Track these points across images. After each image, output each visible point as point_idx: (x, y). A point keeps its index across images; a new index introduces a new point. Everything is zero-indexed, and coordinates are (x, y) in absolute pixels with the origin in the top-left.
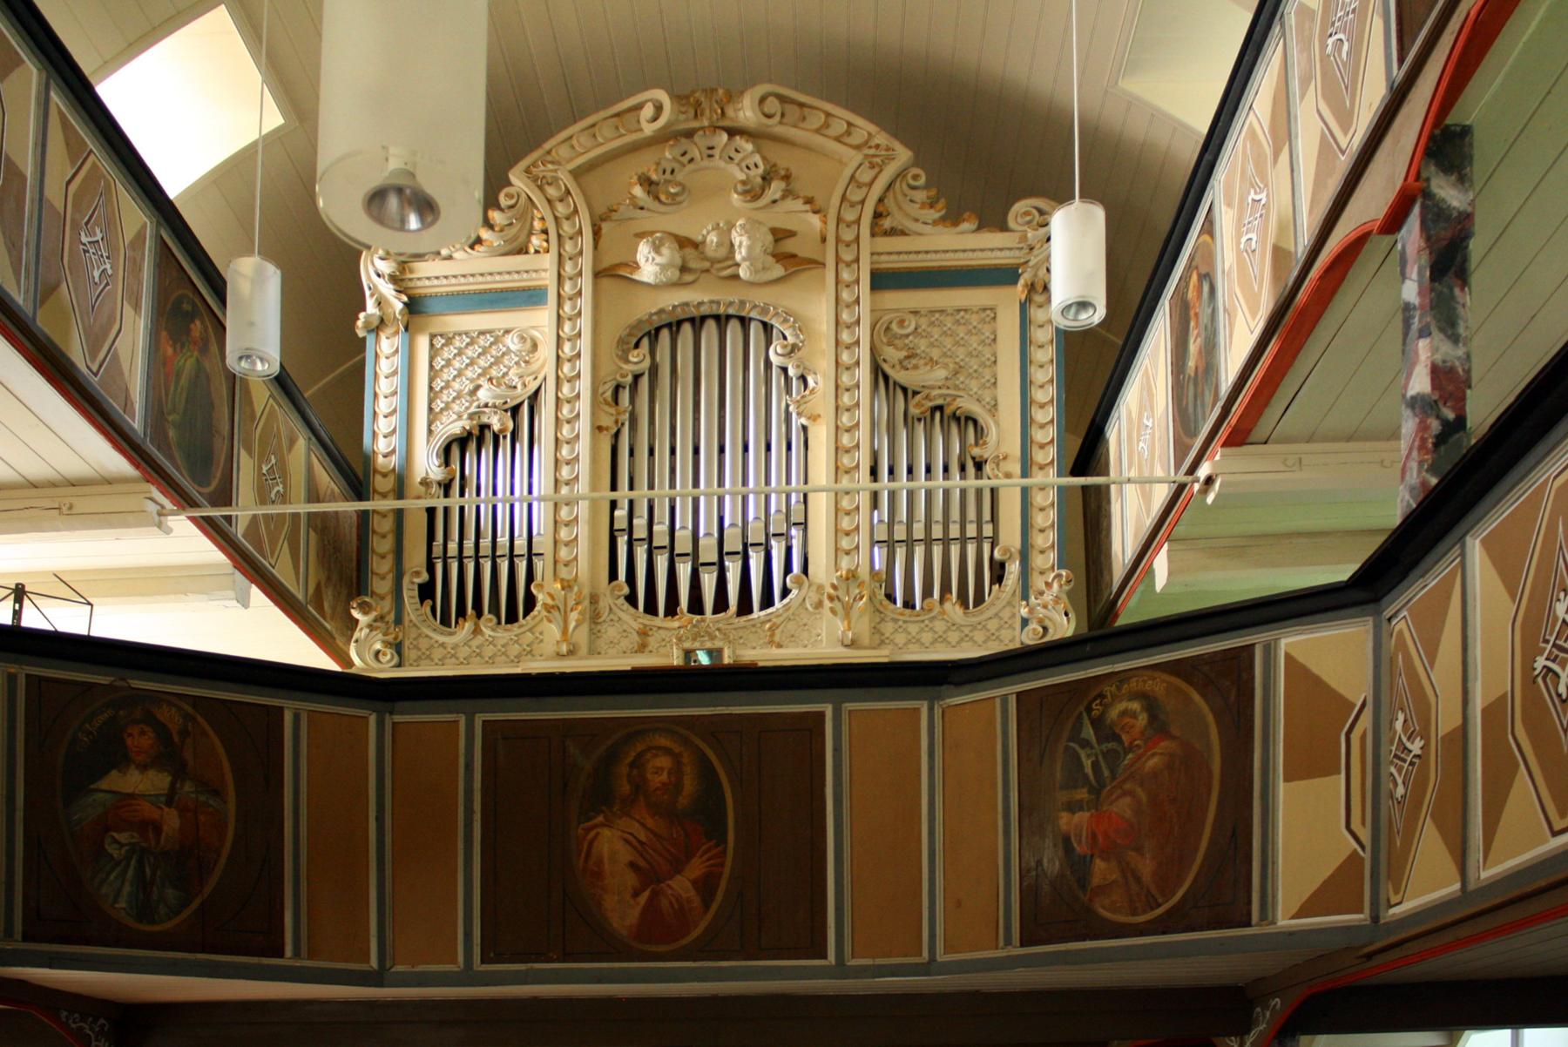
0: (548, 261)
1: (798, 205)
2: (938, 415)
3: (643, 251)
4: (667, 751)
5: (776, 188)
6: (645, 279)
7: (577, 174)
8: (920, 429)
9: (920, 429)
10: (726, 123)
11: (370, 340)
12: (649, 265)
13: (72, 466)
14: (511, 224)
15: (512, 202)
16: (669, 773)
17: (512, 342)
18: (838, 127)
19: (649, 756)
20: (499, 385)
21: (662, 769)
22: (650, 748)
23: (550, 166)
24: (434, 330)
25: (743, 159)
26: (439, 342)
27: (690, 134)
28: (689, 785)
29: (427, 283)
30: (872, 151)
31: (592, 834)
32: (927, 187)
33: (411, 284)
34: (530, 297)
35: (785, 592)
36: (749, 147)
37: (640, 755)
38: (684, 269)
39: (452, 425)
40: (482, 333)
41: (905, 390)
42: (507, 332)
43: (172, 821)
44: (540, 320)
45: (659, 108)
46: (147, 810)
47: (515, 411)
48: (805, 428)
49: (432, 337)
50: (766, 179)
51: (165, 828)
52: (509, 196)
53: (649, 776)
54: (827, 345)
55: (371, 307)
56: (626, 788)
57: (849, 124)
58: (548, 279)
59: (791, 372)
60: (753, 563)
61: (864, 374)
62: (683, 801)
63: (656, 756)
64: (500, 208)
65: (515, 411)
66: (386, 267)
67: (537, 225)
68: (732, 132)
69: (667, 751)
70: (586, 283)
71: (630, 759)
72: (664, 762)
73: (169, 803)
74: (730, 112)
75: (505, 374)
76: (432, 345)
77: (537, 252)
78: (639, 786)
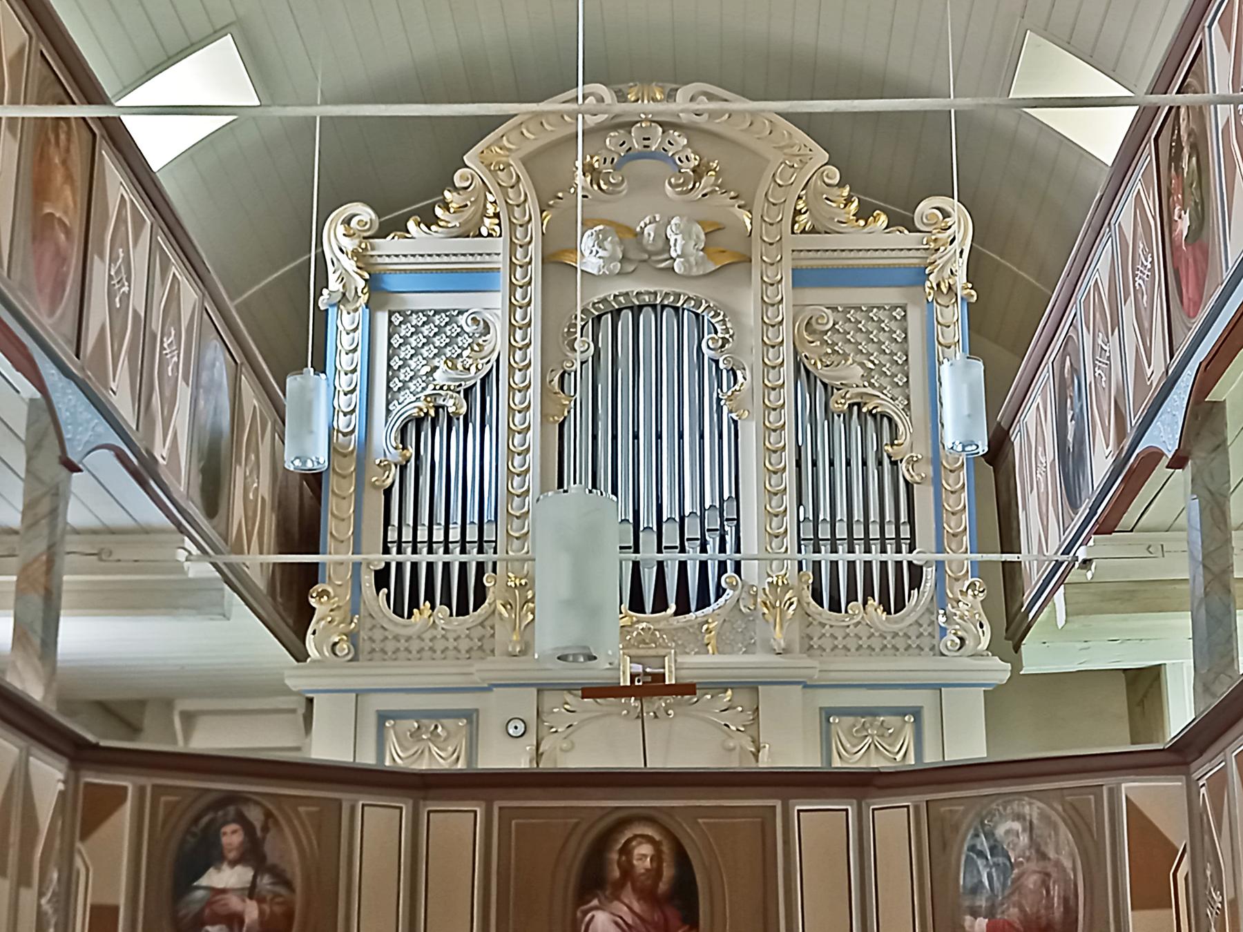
0: (500, 245)
2: (855, 408)
3: (587, 243)
4: (649, 839)
7: (526, 162)
8: (839, 422)
9: (839, 422)
11: (332, 313)
12: (591, 255)
13: (115, 517)
15: (467, 184)
16: (651, 860)
19: (634, 843)
21: (645, 856)
22: (636, 836)
24: (393, 309)
26: (397, 319)
28: (668, 872)
29: (387, 260)
31: (589, 915)
33: (372, 261)
35: (720, 592)
37: (629, 841)
38: (624, 259)
39: (410, 404)
40: (436, 312)
42: (461, 313)
43: (251, 912)
44: (494, 304)
46: (235, 903)
47: (468, 392)
48: (735, 422)
49: (391, 314)
51: (247, 921)
52: (463, 178)
53: (635, 862)
54: (754, 341)
55: (334, 285)
56: (616, 873)
58: (501, 262)
61: (788, 370)
62: (663, 887)
63: (640, 843)
64: (456, 189)
65: (468, 392)
67: (491, 211)
69: (649, 839)
70: (536, 269)
71: (619, 846)
72: (645, 849)
73: (251, 897)
76: (390, 322)
77: (490, 235)
78: (627, 871)
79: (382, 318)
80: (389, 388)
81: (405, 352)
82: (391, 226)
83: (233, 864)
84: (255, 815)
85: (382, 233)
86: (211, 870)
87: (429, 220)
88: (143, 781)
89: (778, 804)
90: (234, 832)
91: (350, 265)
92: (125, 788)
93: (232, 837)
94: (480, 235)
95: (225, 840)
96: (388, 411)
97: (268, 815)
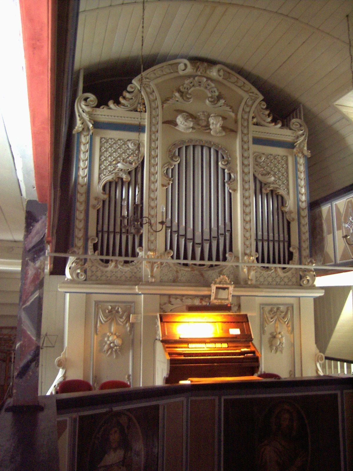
1: (228, 108)
5: (222, 102)
6: (180, 130)
10: (206, 75)
14: (132, 99)
15: (132, 90)
17: (131, 146)
18: (240, 84)
20: (126, 163)
23: (147, 80)
24: (102, 137)
25: (210, 88)
27: (194, 77)
30: (251, 94)
32: (267, 109)
34: (140, 129)
36: (213, 85)
40: (119, 140)
41: (261, 183)
45: (186, 65)
49: (101, 138)
50: (219, 98)
57: (244, 83)
58: (146, 123)
59: (226, 171)
60: (213, 244)
65: (130, 173)
66: (87, 109)
68: (208, 79)
72: (287, 416)
74: (208, 72)
75: (128, 157)
76: (101, 142)
79: (97, 140)
80: (100, 168)
81: (107, 154)
82: (102, 102)
83: (115, 450)
84: (124, 420)
85: (98, 106)
86: (106, 456)
87: (117, 103)
88: (74, 415)
89: (339, 392)
90: (116, 432)
91: (85, 116)
92: (66, 420)
93: (115, 437)
94: (137, 111)
95: (112, 437)
96: (100, 179)
97: (130, 419)
